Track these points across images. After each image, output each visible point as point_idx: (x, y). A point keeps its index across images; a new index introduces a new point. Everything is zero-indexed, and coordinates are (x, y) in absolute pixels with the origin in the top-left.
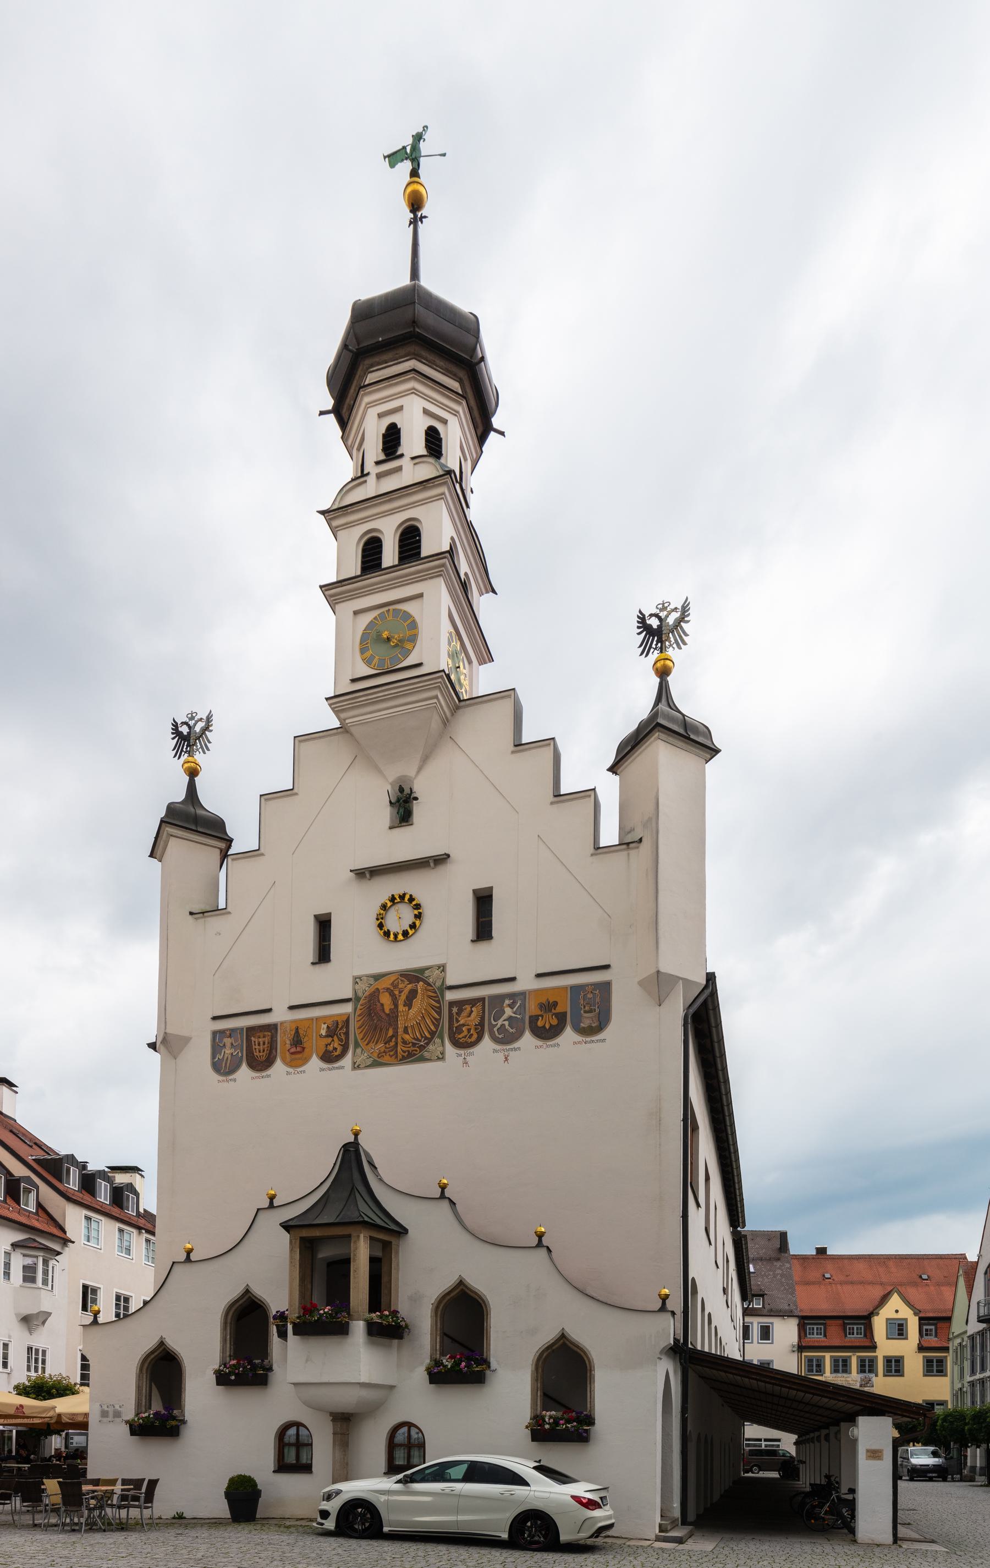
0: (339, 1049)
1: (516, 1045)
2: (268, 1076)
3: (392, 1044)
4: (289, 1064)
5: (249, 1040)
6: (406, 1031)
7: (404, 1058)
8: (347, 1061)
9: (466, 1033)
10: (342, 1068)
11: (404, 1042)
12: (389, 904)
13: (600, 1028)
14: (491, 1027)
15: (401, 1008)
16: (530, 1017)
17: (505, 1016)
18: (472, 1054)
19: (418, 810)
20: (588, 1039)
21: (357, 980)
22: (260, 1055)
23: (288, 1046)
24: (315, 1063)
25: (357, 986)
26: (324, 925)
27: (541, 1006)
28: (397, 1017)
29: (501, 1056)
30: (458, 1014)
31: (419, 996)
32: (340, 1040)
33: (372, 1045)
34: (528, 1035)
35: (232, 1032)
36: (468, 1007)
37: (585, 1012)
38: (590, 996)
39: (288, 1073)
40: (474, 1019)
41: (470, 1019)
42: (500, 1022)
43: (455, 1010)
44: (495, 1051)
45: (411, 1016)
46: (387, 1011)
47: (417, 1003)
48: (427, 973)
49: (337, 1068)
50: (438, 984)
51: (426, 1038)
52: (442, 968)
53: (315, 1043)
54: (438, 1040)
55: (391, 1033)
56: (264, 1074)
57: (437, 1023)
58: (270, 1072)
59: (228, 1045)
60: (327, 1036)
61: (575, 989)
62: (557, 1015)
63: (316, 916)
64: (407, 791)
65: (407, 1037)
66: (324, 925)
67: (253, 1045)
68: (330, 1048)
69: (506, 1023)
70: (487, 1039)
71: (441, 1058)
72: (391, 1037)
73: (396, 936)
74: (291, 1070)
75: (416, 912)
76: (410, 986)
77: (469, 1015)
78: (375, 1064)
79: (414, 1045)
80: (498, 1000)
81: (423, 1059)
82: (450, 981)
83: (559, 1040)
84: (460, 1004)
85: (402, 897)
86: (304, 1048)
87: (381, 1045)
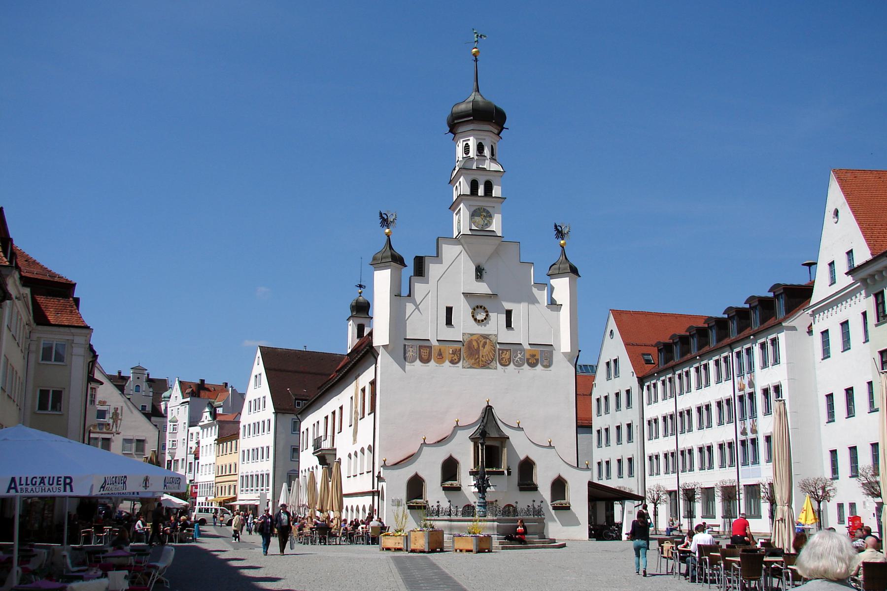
19: (485, 275)
22: (425, 355)
24: (447, 363)
26: (449, 310)
40: (507, 356)
41: (506, 356)
45: (485, 351)
47: (487, 347)
52: (496, 336)
57: (494, 355)
66: (449, 310)
71: (496, 368)
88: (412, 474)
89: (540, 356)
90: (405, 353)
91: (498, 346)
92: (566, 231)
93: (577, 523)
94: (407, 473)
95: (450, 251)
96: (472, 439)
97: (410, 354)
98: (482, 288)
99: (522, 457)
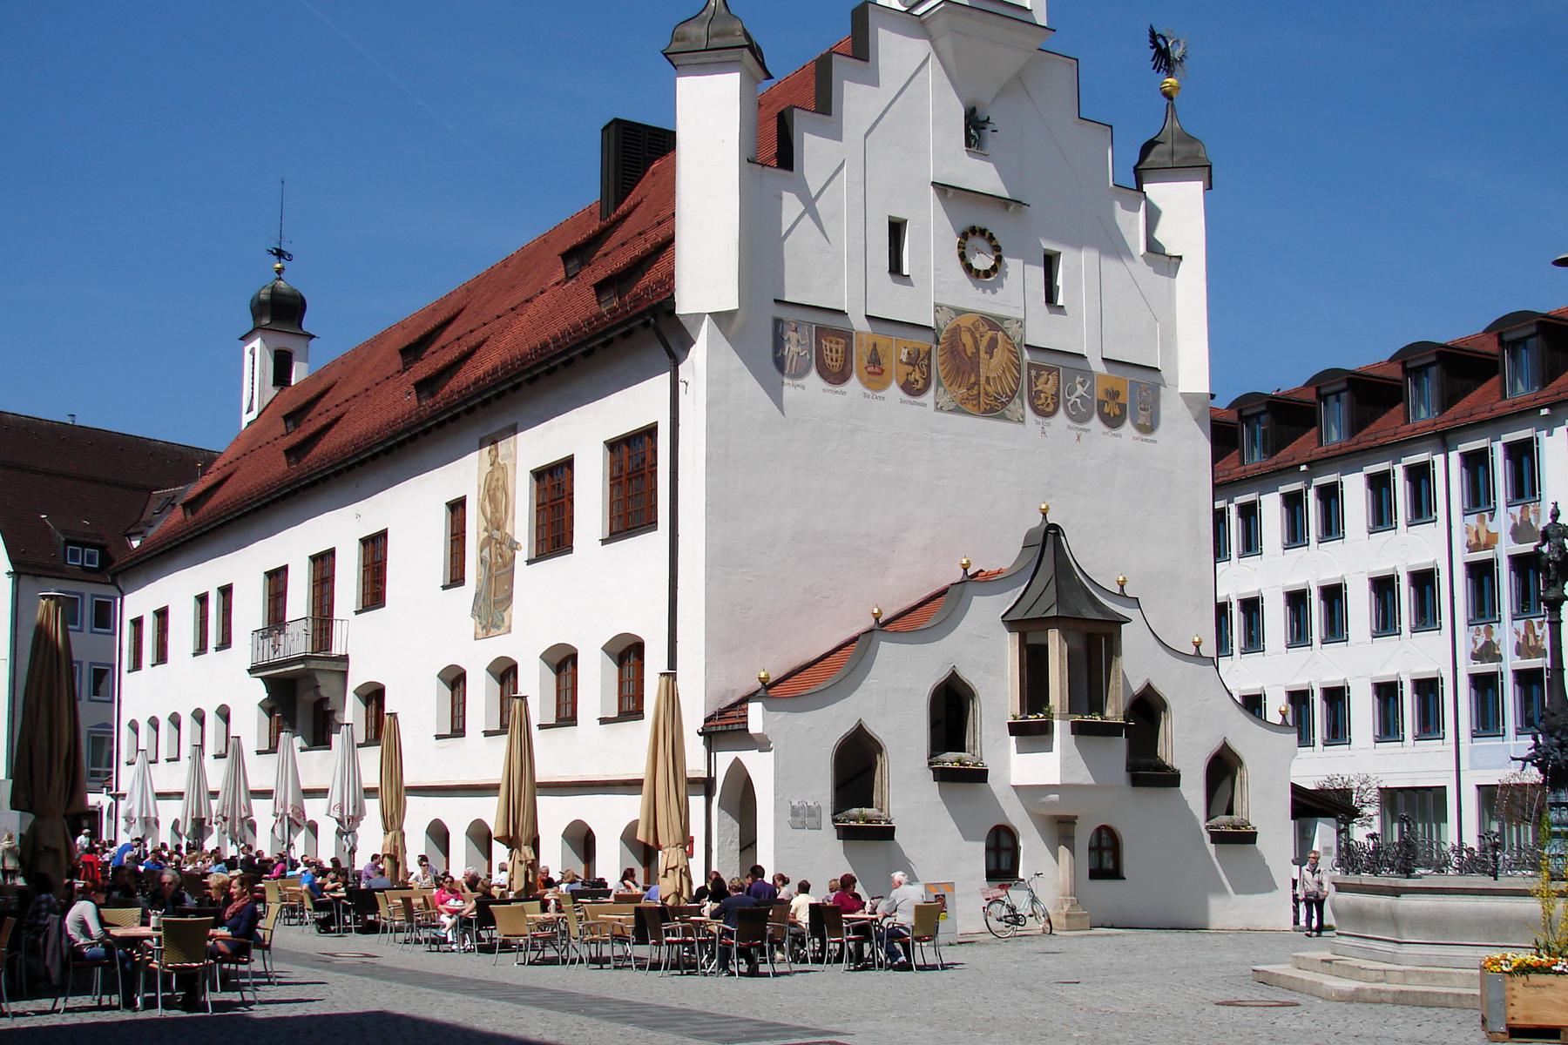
0: (921, 382)
2: (844, 393)
4: (867, 385)
5: (818, 343)
7: (985, 411)
8: (929, 397)
11: (987, 394)
15: (982, 354)
24: (894, 391)
26: (896, 229)
29: (1074, 433)
30: (1037, 377)
33: (955, 387)
34: (1096, 417)
39: (865, 396)
40: (1049, 388)
42: (1073, 398)
43: (1033, 373)
45: (993, 366)
50: (1017, 339)
55: (973, 380)
56: (838, 388)
57: (1017, 380)
59: (794, 341)
66: (896, 229)
68: (911, 378)
70: (1061, 409)
71: (1021, 421)
76: (990, 333)
78: (957, 410)
81: (1003, 418)
83: (1121, 431)
84: (1039, 368)
88: (846, 727)
89: (1127, 397)
90: (778, 342)
91: (1027, 356)
92: (1176, 53)
93: (1268, 885)
94: (826, 727)
95: (896, 51)
96: (1011, 624)
97: (791, 349)
98: (983, 176)
99: (1137, 687)
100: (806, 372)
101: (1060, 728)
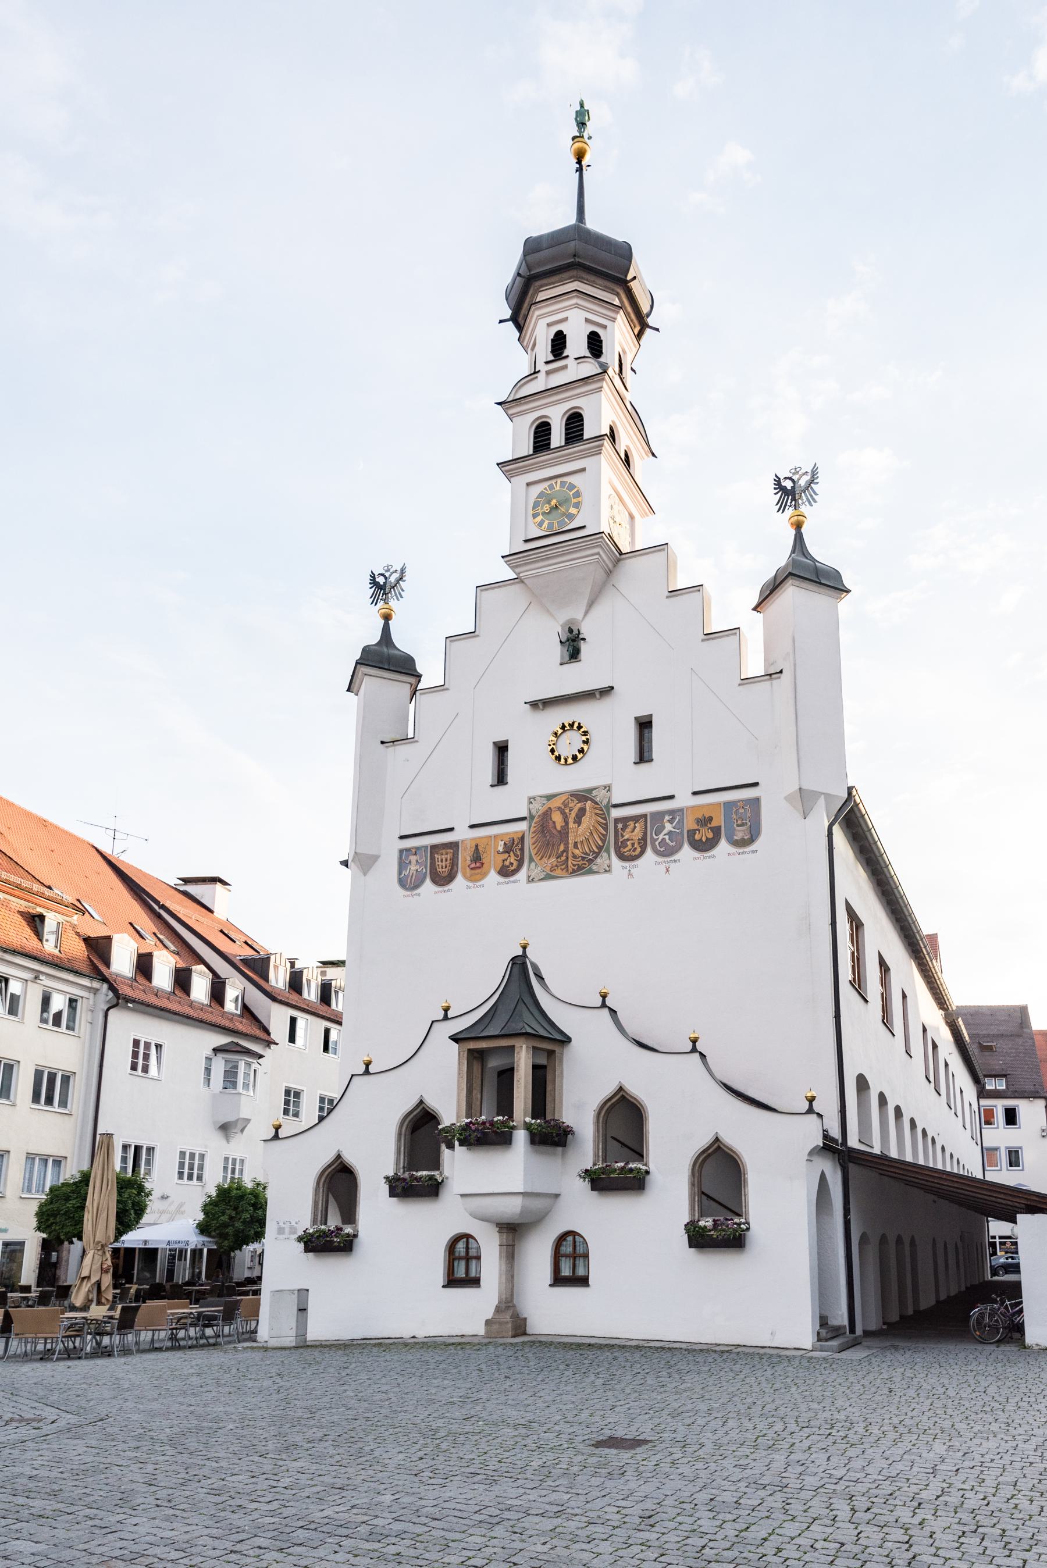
0: (515, 864)
1: (675, 857)
2: (450, 890)
3: (563, 858)
5: (432, 858)
6: (576, 846)
7: (574, 871)
8: (522, 875)
9: (630, 847)
10: (518, 881)
11: (575, 857)
12: (560, 731)
13: (752, 840)
14: (653, 841)
15: (571, 825)
16: (688, 831)
17: (665, 831)
18: (636, 866)
20: (741, 850)
21: (531, 800)
22: (442, 870)
23: (469, 862)
24: (493, 876)
25: (531, 806)
26: (502, 749)
27: (698, 821)
28: (568, 833)
29: (663, 868)
30: (623, 829)
31: (588, 814)
32: (516, 856)
33: (545, 860)
34: (686, 848)
35: (416, 850)
36: (632, 823)
37: (738, 826)
38: (741, 811)
39: (468, 887)
40: (637, 834)
41: (634, 834)
42: (661, 837)
43: (620, 826)
44: (657, 863)
45: (579, 833)
46: (559, 828)
47: (585, 820)
48: (594, 793)
49: (513, 882)
50: (605, 802)
51: (594, 852)
52: (608, 788)
53: (493, 859)
54: (604, 854)
55: (562, 848)
56: (446, 888)
57: (604, 838)
58: (452, 886)
59: (414, 862)
60: (503, 853)
61: (728, 805)
62: (712, 829)
63: (494, 743)
64: (575, 632)
65: (576, 852)
66: (502, 749)
67: (438, 862)
68: (507, 863)
69: (667, 837)
71: (608, 870)
72: (564, 851)
73: (566, 760)
74: (471, 884)
75: (584, 738)
77: (633, 831)
78: (548, 877)
79: (583, 859)
80: (659, 816)
81: (591, 872)
82: (614, 802)
83: (714, 852)
84: (625, 820)
85: (572, 725)
86: (483, 864)
87: (553, 860)
100: (422, 882)
101: (521, 1136)
